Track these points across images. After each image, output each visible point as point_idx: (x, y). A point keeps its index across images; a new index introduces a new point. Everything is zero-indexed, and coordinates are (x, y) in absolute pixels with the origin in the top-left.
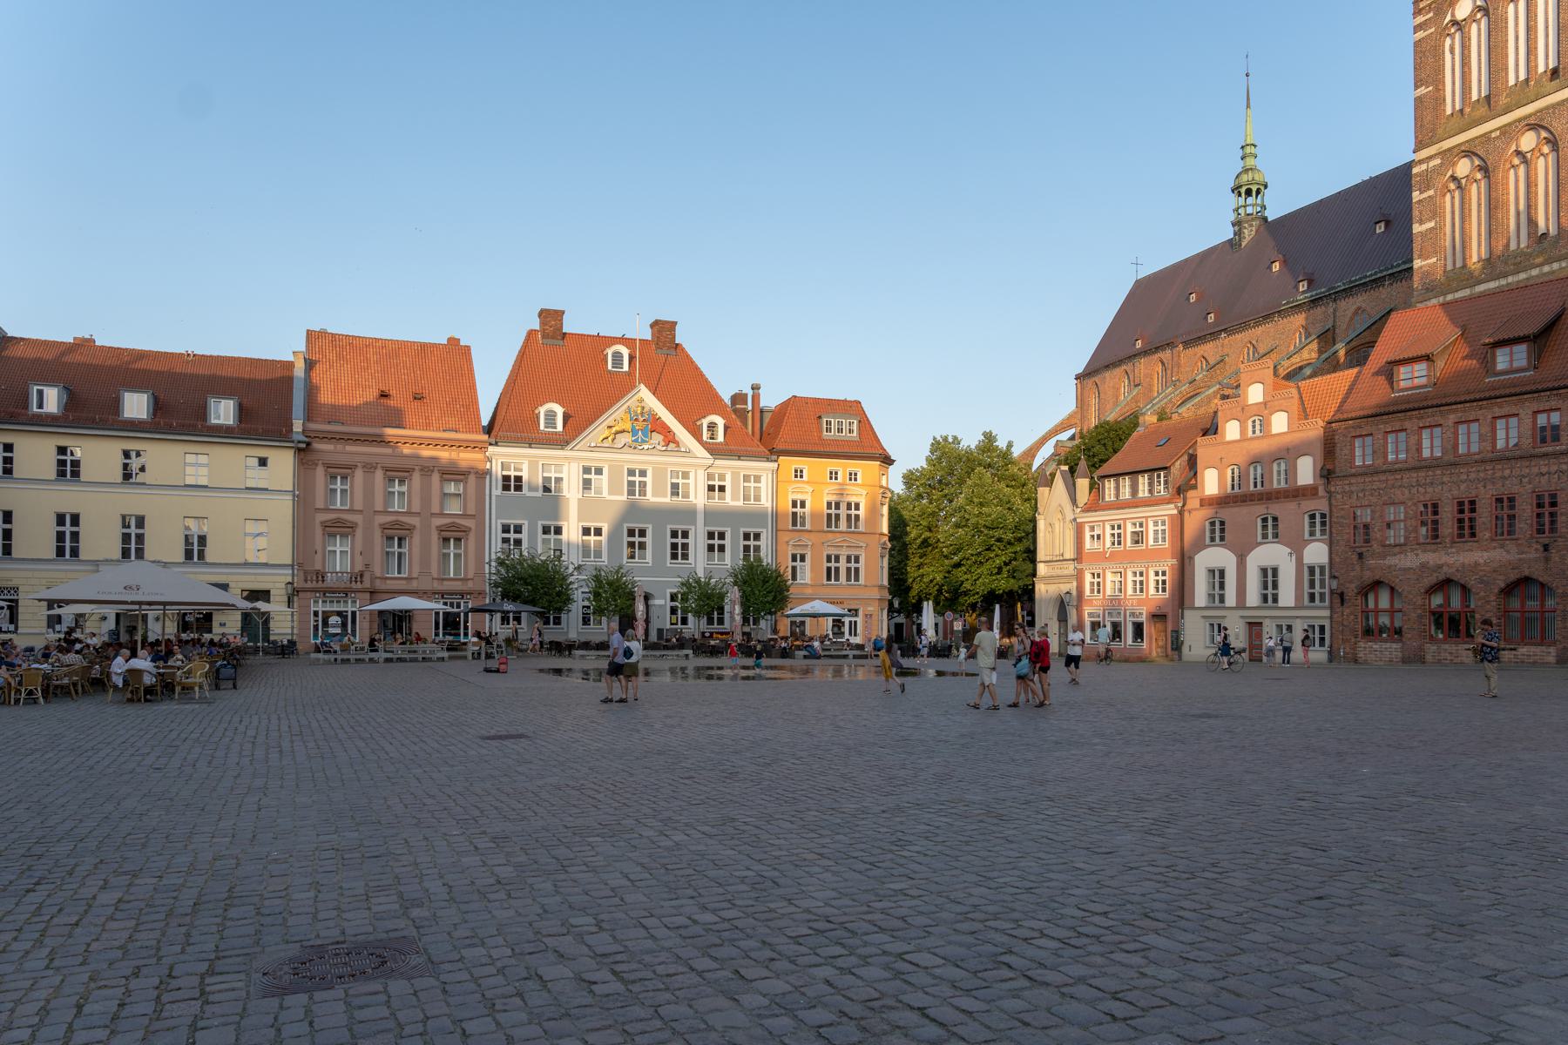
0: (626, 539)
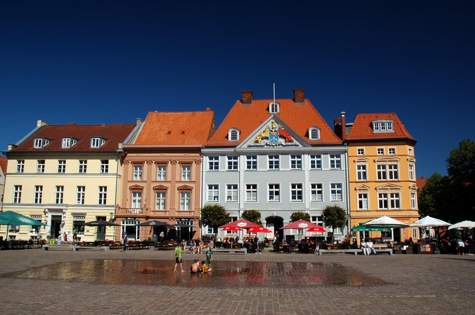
0: (268, 189)
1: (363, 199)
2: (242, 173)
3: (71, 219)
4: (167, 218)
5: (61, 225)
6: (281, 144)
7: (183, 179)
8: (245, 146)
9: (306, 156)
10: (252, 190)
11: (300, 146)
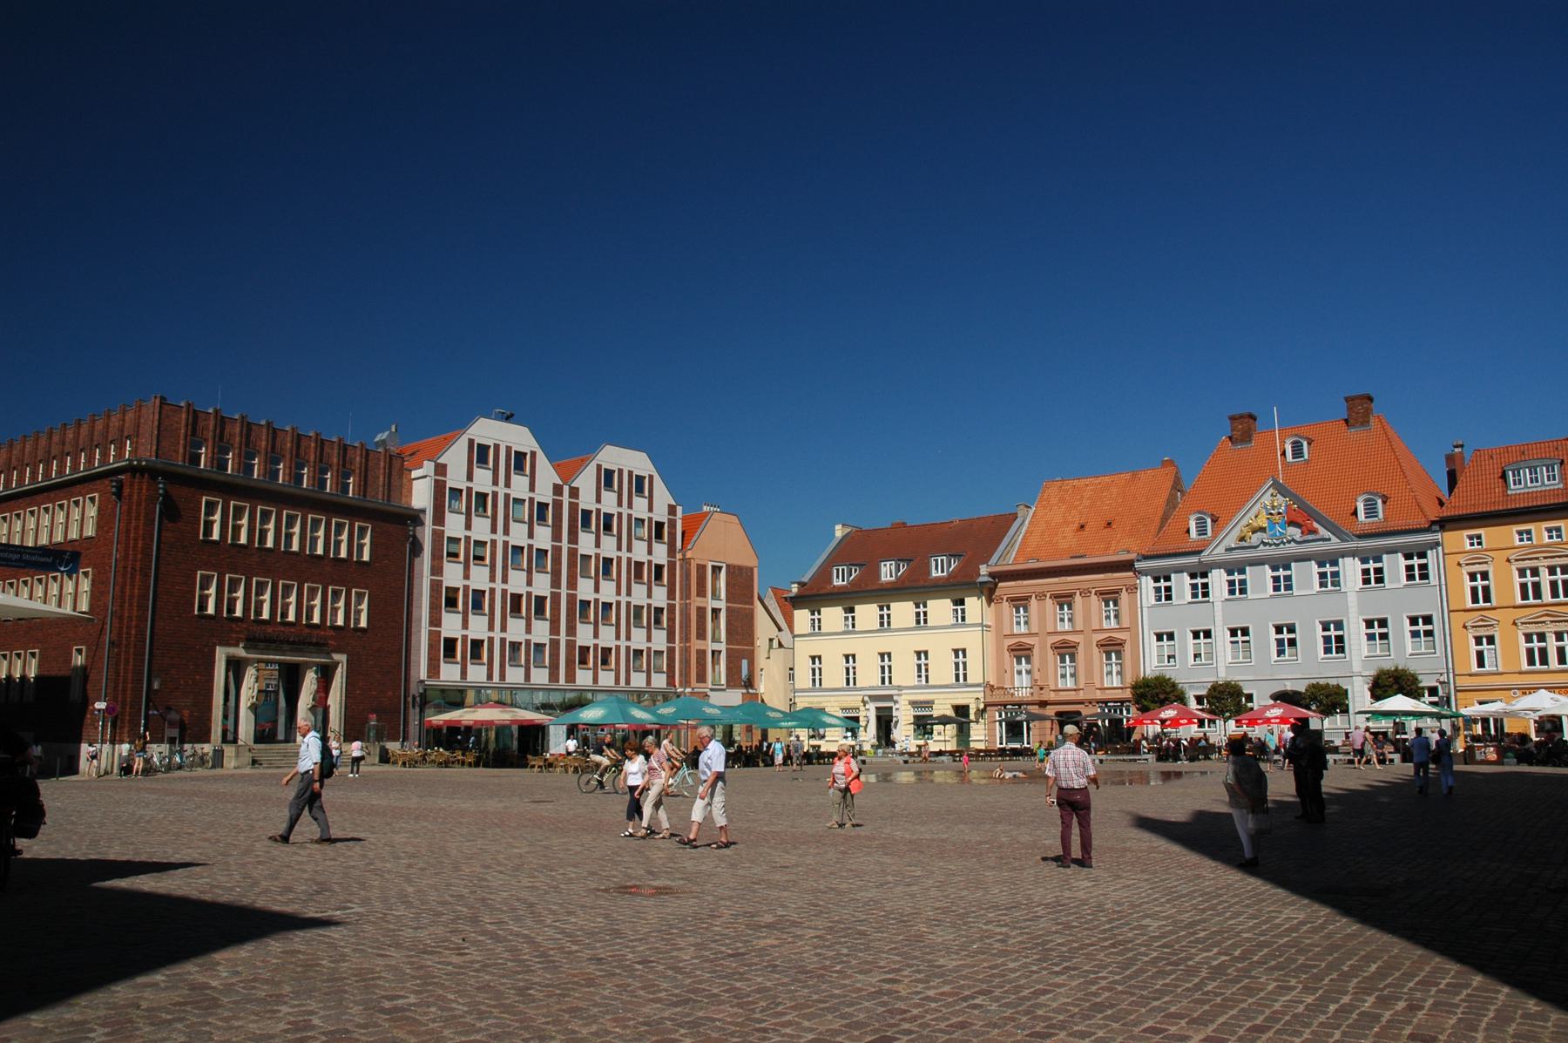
0: (1273, 635)
1: (1485, 646)
2: (1218, 606)
3: (909, 713)
4: (1081, 703)
5: (892, 724)
6: (1293, 540)
7: (1105, 626)
8: (1221, 549)
9: (1348, 560)
10: (1240, 638)
11: (1335, 540)
